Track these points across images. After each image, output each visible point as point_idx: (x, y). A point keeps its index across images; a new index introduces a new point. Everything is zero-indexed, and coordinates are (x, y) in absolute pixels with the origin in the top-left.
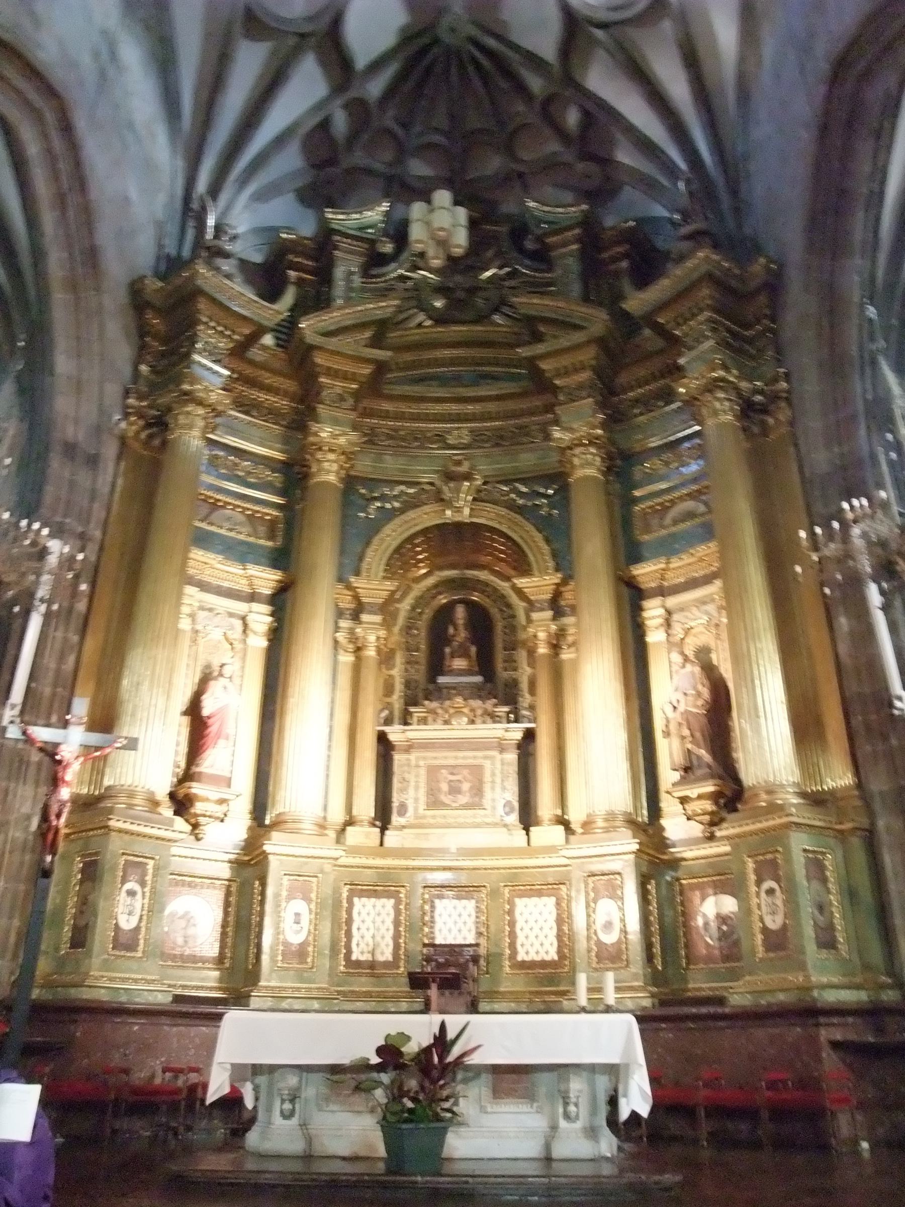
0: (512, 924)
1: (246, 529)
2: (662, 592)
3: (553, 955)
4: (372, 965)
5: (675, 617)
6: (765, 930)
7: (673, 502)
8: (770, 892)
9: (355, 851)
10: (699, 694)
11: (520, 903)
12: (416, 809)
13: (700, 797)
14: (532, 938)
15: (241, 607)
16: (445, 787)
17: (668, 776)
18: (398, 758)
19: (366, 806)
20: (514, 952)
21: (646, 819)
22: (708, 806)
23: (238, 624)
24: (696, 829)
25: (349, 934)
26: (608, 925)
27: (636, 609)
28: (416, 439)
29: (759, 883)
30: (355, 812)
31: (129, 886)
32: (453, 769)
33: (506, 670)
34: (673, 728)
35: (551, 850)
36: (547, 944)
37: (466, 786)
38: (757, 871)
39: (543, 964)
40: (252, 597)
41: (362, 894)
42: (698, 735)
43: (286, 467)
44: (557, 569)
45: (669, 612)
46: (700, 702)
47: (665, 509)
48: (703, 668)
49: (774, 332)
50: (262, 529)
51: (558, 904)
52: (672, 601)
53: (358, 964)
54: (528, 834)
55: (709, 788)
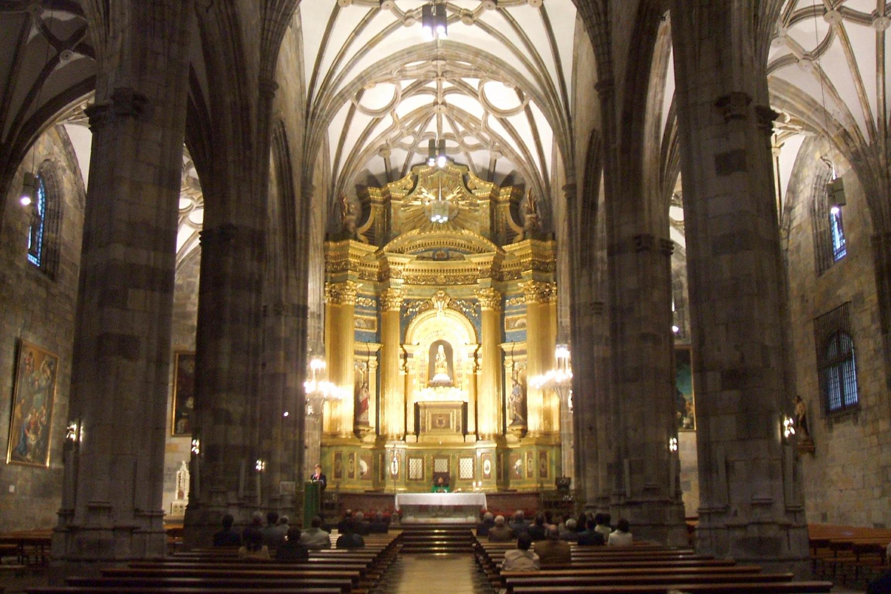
0: (459, 467)
1: (365, 326)
2: (512, 353)
3: (471, 476)
4: (416, 480)
5: (516, 364)
6: (528, 472)
7: (519, 318)
8: (530, 461)
9: (410, 444)
10: (519, 396)
11: (461, 460)
12: (428, 429)
13: (517, 430)
14: (465, 471)
15: (366, 358)
16: (437, 422)
17: (509, 422)
18: (421, 412)
19: (411, 428)
20: (459, 476)
21: (502, 433)
22: (519, 432)
23: (365, 364)
24: (516, 439)
25: (409, 471)
26: (487, 469)
27: (503, 360)
28: (424, 281)
29: (528, 458)
30: (408, 430)
31: (350, 460)
32: (440, 416)
33: (457, 369)
34: (511, 406)
35: (471, 444)
36: (470, 473)
37: (444, 422)
38: (527, 456)
39: (468, 479)
40: (369, 354)
41: (412, 458)
42: (518, 410)
43: (377, 298)
44: (477, 343)
45: (514, 362)
46: (519, 399)
47: (516, 320)
48: (522, 387)
49: (555, 262)
50: (369, 325)
51: (473, 461)
52: (515, 358)
53: (411, 479)
54: (465, 437)
55: (520, 427)
